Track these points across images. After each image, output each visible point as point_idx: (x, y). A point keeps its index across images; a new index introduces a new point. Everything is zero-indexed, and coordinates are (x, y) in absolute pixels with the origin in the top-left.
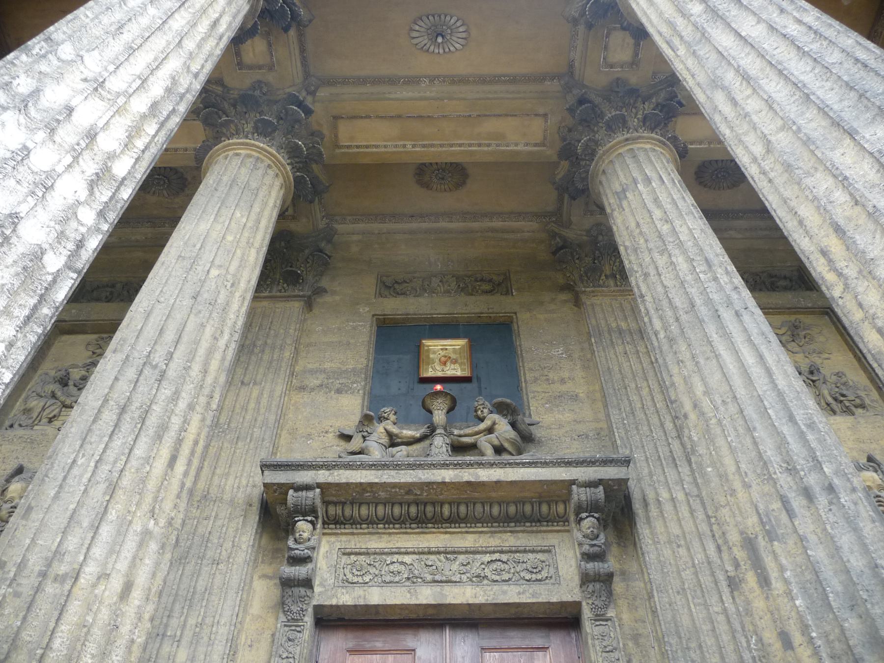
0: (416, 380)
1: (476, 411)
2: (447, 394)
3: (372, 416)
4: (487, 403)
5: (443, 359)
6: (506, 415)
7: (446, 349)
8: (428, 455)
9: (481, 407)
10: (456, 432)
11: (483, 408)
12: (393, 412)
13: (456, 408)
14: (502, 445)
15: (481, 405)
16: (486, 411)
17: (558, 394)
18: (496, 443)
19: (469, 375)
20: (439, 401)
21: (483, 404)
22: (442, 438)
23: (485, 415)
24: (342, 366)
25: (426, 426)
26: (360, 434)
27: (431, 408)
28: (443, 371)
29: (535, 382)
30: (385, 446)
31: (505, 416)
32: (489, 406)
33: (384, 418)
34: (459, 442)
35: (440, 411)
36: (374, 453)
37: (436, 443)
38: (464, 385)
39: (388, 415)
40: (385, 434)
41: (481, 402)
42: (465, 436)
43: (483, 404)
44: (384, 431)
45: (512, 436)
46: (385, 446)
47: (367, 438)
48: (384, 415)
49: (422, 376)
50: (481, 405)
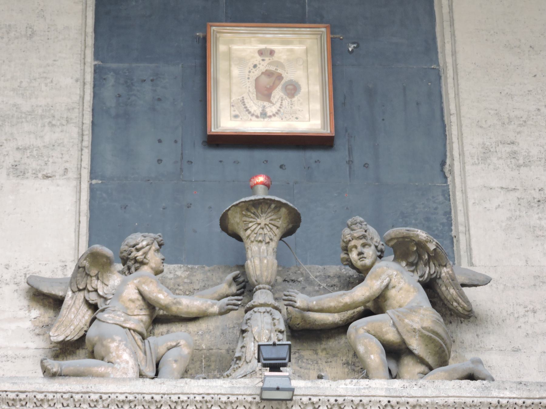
0: (199, 139)
1: (346, 250)
2: (280, 205)
3: (108, 258)
4: (372, 231)
5: (265, 80)
6: (416, 265)
7: (272, 52)
8: (239, 358)
9: (359, 243)
10: (301, 300)
11: (364, 245)
12: (155, 246)
13: (298, 231)
14: (404, 342)
15: (359, 238)
16: (370, 252)
17: (537, 196)
18: (391, 336)
19: (327, 131)
20: (263, 220)
21: (364, 237)
22: (268, 318)
23: (368, 262)
24: (19, 101)
25: (230, 277)
26: (81, 295)
27: (242, 234)
28: (264, 115)
29: (484, 159)
30: (140, 334)
31: (413, 265)
32: (377, 238)
33: (136, 260)
34: (304, 319)
35: (263, 247)
36: (119, 357)
37: (255, 329)
38: (313, 155)
39: (145, 254)
40: (141, 303)
41: (358, 232)
42: (321, 311)
43: (364, 237)
44: (135, 295)
45: (428, 323)
46: (140, 334)
47: (99, 315)
48: (134, 254)
49: (214, 130)
50: (359, 238)
